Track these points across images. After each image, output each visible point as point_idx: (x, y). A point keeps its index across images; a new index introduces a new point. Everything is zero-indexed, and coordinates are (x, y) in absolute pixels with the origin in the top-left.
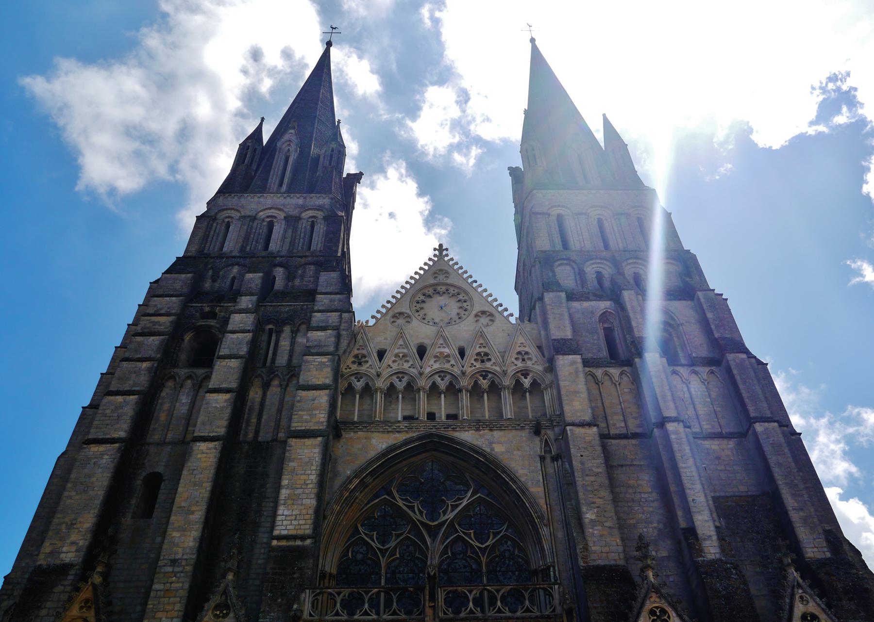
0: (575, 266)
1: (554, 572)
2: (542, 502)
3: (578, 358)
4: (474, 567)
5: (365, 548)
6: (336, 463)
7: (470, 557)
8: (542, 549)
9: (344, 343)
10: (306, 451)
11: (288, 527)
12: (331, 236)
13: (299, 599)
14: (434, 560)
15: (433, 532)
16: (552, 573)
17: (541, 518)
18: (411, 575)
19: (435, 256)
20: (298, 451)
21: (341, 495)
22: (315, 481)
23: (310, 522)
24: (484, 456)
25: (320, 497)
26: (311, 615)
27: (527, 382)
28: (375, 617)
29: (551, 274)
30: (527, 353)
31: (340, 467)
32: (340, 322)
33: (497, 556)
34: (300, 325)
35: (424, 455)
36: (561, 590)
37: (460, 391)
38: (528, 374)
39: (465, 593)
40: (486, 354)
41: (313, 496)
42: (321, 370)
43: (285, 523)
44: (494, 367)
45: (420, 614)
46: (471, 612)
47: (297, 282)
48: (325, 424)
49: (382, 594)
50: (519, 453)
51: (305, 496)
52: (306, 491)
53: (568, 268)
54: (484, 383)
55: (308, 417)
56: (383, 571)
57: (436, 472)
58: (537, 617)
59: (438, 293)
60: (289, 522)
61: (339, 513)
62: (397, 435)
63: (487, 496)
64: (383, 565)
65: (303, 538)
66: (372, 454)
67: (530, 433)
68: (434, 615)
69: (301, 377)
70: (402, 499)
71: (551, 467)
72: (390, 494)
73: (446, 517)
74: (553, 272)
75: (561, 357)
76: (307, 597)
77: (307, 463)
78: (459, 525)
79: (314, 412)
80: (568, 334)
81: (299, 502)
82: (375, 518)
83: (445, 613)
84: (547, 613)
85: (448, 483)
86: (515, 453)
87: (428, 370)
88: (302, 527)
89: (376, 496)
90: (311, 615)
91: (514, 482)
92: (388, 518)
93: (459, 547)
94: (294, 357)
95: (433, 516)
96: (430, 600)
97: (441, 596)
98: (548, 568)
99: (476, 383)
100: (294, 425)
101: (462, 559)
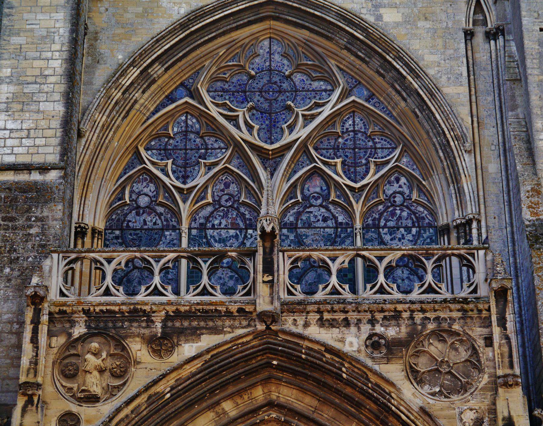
1: (479, 229)
2: (464, 112)
4: (341, 219)
5: (152, 187)
6: (96, 39)
7: (334, 203)
8: (460, 192)
10: (40, 16)
13: (41, 268)
14: (271, 208)
15: (271, 160)
16: (475, 232)
17: (460, 139)
18: (232, 232)
20: (26, 16)
22: (60, 71)
23: (55, 141)
24: (364, 30)
25: (70, 99)
26: (62, 294)
28: (172, 297)
31: (103, 47)
33: (380, 203)
35: (255, 28)
36: (489, 257)
39: (324, 261)
41: (57, 97)
43: (9, 142)
45: (248, 294)
46: (335, 292)
49: (184, 262)
50: (428, 25)
52: (45, 88)
56: (185, 226)
57: (277, 57)
58: (445, 301)
60: (16, 142)
61: (106, 127)
63: (367, 100)
64: (185, 215)
65: (43, 169)
66: (161, 24)
68: (271, 294)
70: (217, 105)
71: (484, 50)
72: (194, 94)
73: (293, 136)
76: (54, 266)
77: (43, 38)
78: (316, 149)
81: (33, 107)
82: (170, 138)
83: (290, 293)
84: (463, 295)
85: (298, 78)
86: (420, 24)
88: (41, 150)
89: (170, 99)
90: (62, 294)
91: (417, 76)
92: (192, 136)
93: (316, 186)
95: (271, 131)
96: (265, 271)
97: (283, 265)
98: (469, 222)
101: (321, 206)
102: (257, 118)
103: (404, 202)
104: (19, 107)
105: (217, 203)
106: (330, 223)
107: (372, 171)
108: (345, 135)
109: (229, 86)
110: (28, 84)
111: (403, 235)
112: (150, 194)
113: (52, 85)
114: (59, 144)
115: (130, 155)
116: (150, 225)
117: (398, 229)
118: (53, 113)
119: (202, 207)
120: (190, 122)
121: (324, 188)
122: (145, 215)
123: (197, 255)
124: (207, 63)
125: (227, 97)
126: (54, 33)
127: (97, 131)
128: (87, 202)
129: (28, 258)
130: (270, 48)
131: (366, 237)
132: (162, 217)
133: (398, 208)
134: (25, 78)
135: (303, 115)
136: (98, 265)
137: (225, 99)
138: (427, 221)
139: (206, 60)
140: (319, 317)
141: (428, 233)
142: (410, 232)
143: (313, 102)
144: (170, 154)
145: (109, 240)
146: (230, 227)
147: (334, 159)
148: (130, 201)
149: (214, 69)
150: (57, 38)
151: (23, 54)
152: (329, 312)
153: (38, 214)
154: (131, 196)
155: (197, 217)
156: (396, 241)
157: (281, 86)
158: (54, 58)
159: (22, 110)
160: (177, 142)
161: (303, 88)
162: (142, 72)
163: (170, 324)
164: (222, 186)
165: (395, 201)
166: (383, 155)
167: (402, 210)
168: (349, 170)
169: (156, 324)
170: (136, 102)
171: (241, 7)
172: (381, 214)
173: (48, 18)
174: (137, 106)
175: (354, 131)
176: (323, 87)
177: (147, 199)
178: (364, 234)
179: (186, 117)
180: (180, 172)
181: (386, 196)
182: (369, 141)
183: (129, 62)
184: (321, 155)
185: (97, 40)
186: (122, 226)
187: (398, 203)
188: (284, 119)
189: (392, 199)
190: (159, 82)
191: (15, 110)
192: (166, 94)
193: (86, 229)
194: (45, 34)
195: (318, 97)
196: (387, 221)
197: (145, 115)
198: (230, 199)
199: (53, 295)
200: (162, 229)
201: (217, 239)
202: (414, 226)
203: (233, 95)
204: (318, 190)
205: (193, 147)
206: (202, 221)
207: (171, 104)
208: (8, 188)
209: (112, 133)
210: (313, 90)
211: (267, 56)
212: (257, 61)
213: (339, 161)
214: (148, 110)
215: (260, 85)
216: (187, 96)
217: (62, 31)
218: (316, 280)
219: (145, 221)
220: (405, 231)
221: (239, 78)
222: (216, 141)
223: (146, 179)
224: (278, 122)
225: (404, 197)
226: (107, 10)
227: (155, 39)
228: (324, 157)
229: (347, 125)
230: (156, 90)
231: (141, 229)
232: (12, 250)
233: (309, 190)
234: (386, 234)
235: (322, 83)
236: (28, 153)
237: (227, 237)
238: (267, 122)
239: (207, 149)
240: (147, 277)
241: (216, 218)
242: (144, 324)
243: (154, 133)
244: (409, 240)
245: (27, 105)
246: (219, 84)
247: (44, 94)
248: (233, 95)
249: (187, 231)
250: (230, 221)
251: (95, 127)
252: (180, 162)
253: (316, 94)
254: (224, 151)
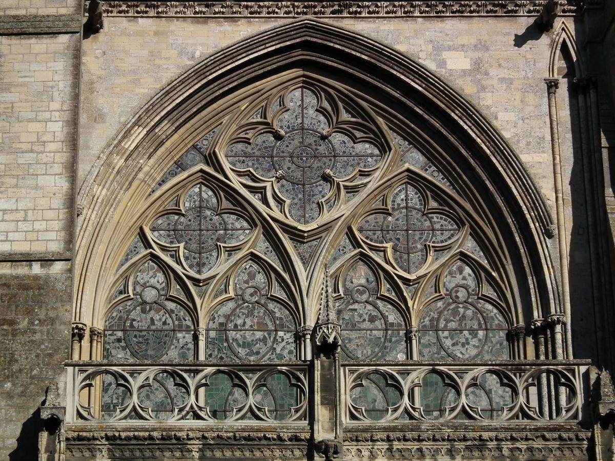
5: (160, 277)
7: (384, 299)
11: (11, 236)
18: (259, 335)
20: (17, 66)
21: (108, 164)
23: (57, 225)
41: (58, 169)
51: (40, 170)
52: (44, 158)
60: (11, 226)
65: (46, 261)
66: (171, 71)
70: (240, 174)
72: (212, 159)
73: (334, 214)
81: (30, 182)
88: (42, 236)
89: (180, 166)
92: (208, 213)
102: (287, 191)
103: (468, 297)
104: (13, 181)
105: (240, 298)
106: (379, 324)
107: (430, 259)
108: (396, 213)
109: (253, 149)
110: (23, 152)
111: (467, 339)
112: (159, 286)
113: (52, 154)
114: (63, 229)
115: (133, 237)
116: (159, 324)
117: (461, 331)
118: (54, 190)
119: (222, 303)
120: (204, 196)
121: (372, 278)
122: (152, 312)
123: (240, 370)
124: (225, 120)
125: (250, 164)
126: (52, 87)
127: (96, 208)
128: (84, 297)
129: (32, 370)
130: (302, 100)
131: (422, 341)
132: (174, 315)
133: (461, 306)
134: (19, 146)
135: (346, 187)
136: (122, 382)
137: (248, 166)
138: (496, 322)
139: (224, 116)
140: (387, 447)
141: (497, 337)
142: (475, 336)
143: (357, 170)
144: (182, 236)
145: (109, 343)
146: (256, 327)
147: (382, 242)
148: (134, 295)
149: (234, 127)
150: (56, 94)
151: (16, 115)
152: (399, 440)
153: (42, 316)
154: (134, 289)
155: (216, 316)
156: (459, 347)
157: (317, 149)
158: (53, 119)
159: (16, 186)
160: (190, 220)
161: (344, 152)
162: (148, 133)
163: (208, 454)
164: (246, 278)
165: (457, 297)
166: (444, 238)
167: (466, 308)
168: (401, 258)
169: (194, 453)
170: (140, 169)
172: (440, 313)
173: (44, 68)
174: (141, 175)
175: (407, 208)
176: (369, 151)
177: (154, 292)
178: (420, 338)
179: (200, 188)
180: (194, 258)
181: (447, 290)
182: (425, 220)
183: (133, 120)
184: (367, 238)
185: (92, 92)
186: (124, 325)
187: (461, 299)
188: (321, 192)
189: (454, 295)
190: (168, 144)
191: (8, 186)
192: (175, 159)
193: (84, 330)
194: (41, 88)
195: (362, 165)
196: (448, 321)
197: (149, 185)
198: (255, 293)
199: (70, 419)
200: (174, 330)
201: (241, 343)
202: (480, 328)
203: (258, 160)
204: (363, 281)
205: (210, 228)
206: (222, 320)
207: (180, 172)
208: (5, 285)
209: (112, 210)
210: (357, 155)
211: (298, 110)
212: (286, 117)
213: (389, 245)
214: (154, 180)
215: (290, 149)
216: (201, 162)
217: (61, 85)
218: (361, 395)
219: (152, 319)
220: (470, 334)
221: (265, 138)
222: (238, 219)
223: (152, 268)
224: (313, 195)
225: (468, 292)
226: (104, 53)
227: (165, 90)
228: (371, 240)
229: (398, 200)
230: (163, 154)
231: (148, 330)
232: (13, 360)
233: (352, 282)
234: (446, 338)
235: (367, 146)
236: (26, 240)
237: (252, 341)
238: (300, 196)
239: (226, 230)
240: (157, 389)
241: (239, 317)
242: (178, 454)
243: (161, 209)
244: (474, 346)
245: (22, 179)
246: (240, 146)
247: (42, 166)
248: (258, 160)
249: (204, 333)
250: (256, 320)
251: (94, 202)
252: (194, 246)
253: (360, 159)
254: (247, 232)
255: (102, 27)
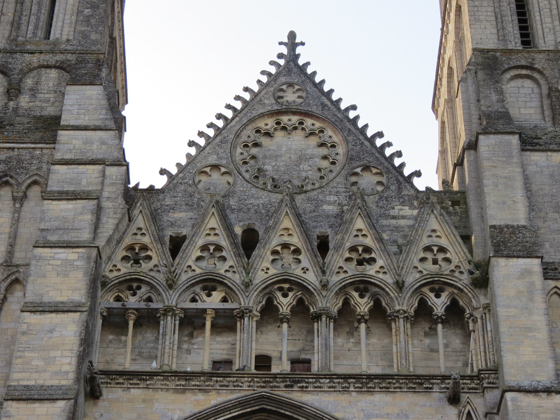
0: (542, 82)
3: (535, 264)
9: (109, 224)
12: (87, 11)
19: (280, 56)
27: (439, 304)
29: (494, 97)
30: (442, 250)
32: (103, 183)
34: (29, 186)
37: (317, 317)
38: (442, 290)
40: (367, 250)
42: (66, 276)
44: (381, 276)
47: (24, 101)
48: (72, 376)
53: (528, 83)
54: (363, 305)
55: (41, 363)
59: (284, 128)
62: (200, 396)
67: (440, 399)
69: (30, 287)
74: (501, 92)
75: (502, 262)
79: (52, 354)
80: (520, 216)
87: (260, 277)
94: (17, 248)
99: (346, 303)
100: (15, 376)
171: (234, 414)
255: (101, 394)
